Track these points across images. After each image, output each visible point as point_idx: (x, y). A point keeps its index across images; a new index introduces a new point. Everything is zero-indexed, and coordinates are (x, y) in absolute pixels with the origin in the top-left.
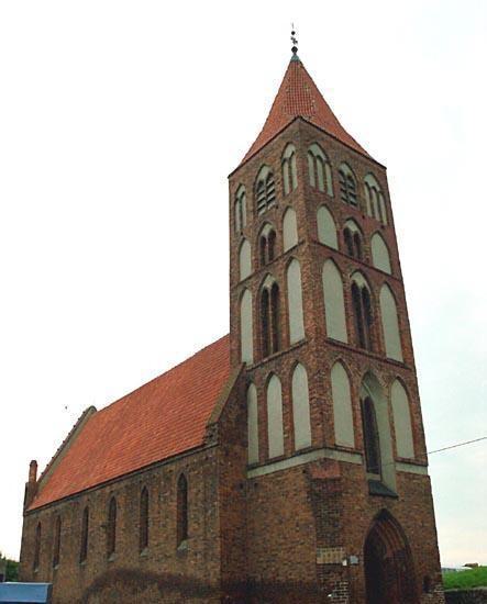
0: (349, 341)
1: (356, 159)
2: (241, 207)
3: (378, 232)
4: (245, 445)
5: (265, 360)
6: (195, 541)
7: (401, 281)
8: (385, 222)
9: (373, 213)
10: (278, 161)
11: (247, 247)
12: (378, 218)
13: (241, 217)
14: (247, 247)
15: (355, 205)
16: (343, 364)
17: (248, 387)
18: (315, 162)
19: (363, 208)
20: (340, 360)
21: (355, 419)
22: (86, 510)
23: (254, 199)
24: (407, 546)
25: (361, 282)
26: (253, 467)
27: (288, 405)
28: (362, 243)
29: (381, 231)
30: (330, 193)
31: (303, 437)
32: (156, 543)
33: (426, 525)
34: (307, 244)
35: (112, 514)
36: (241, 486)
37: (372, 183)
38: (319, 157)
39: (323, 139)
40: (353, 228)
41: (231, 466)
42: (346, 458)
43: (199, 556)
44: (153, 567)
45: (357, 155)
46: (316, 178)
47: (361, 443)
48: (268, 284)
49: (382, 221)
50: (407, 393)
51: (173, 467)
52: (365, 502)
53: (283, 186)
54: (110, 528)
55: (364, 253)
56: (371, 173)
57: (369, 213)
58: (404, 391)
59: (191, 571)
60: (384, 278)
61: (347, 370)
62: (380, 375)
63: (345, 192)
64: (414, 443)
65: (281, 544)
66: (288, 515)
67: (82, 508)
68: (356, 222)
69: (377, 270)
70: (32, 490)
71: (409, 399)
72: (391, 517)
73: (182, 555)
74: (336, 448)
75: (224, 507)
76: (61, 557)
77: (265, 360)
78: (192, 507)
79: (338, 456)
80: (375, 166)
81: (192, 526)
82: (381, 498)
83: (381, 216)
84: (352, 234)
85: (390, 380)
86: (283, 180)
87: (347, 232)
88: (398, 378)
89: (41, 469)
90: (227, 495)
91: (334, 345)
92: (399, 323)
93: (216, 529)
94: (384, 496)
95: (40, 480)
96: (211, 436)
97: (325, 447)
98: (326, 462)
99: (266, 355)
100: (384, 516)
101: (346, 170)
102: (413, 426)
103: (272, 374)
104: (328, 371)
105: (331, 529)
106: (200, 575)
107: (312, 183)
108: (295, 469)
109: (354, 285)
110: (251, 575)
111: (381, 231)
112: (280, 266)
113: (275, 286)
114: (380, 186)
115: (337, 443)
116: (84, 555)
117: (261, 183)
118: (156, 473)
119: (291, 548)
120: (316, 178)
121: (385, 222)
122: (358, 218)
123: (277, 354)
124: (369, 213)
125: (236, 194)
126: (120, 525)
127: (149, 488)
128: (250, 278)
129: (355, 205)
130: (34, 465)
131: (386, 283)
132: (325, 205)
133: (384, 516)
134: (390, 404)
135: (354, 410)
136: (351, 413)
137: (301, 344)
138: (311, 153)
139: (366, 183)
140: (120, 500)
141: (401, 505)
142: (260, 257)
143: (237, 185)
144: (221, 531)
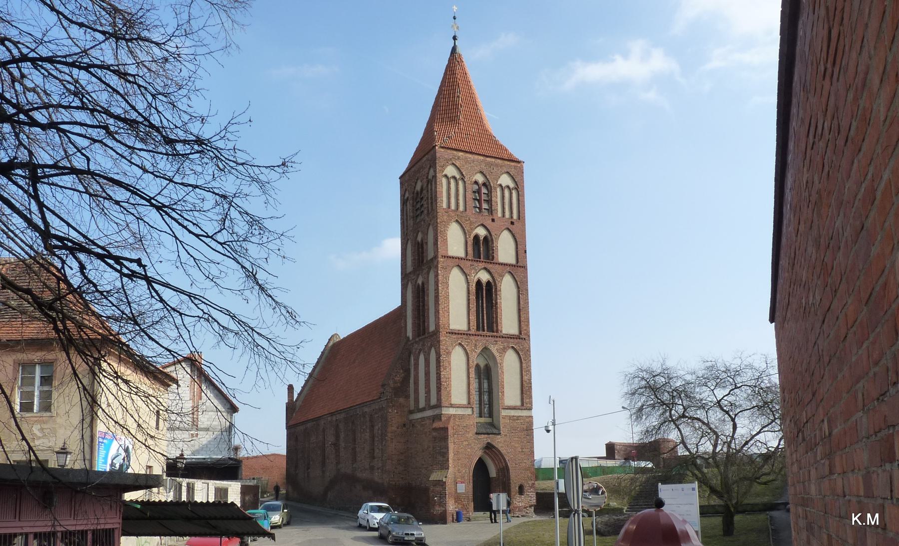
1: (490, 165)
5: (417, 340)
7: (525, 267)
9: (504, 212)
10: (425, 180)
16: (463, 346)
17: (410, 357)
18: (449, 183)
20: (460, 344)
22: (324, 431)
23: (413, 206)
25: (484, 277)
26: (411, 412)
27: (427, 374)
29: (511, 227)
30: (461, 208)
35: (337, 437)
37: (505, 180)
38: (454, 177)
39: (459, 158)
40: (481, 232)
41: (397, 413)
44: (359, 474)
45: (493, 160)
48: (420, 282)
49: (512, 217)
51: (366, 409)
53: (428, 204)
54: (336, 445)
56: (508, 173)
59: (376, 479)
60: (508, 269)
61: (465, 349)
62: (494, 349)
65: (423, 465)
66: (426, 447)
70: (291, 408)
72: (494, 447)
76: (311, 463)
78: (376, 439)
80: (513, 164)
81: (377, 451)
84: (482, 238)
85: (504, 350)
86: (428, 198)
88: (513, 347)
89: (297, 390)
91: (455, 333)
92: (519, 303)
94: (488, 434)
95: (296, 400)
99: (419, 336)
100: (489, 447)
103: (420, 350)
106: (380, 481)
108: (428, 418)
109: (479, 283)
111: (511, 227)
114: (516, 182)
115: (452, 403)
116: (323, 464)
117: (417, 193)
121: (515, 216)
122: (488, 223)
123: (423, 337)
124: (500, 214)
125: (404, 196)
126: (342, 444)
128: (410, 273)
130: (291, 388)
133: (489, 447)
138: (446, 176)
139: (501, 185)
140: (341, 426)
143: (404, 188)
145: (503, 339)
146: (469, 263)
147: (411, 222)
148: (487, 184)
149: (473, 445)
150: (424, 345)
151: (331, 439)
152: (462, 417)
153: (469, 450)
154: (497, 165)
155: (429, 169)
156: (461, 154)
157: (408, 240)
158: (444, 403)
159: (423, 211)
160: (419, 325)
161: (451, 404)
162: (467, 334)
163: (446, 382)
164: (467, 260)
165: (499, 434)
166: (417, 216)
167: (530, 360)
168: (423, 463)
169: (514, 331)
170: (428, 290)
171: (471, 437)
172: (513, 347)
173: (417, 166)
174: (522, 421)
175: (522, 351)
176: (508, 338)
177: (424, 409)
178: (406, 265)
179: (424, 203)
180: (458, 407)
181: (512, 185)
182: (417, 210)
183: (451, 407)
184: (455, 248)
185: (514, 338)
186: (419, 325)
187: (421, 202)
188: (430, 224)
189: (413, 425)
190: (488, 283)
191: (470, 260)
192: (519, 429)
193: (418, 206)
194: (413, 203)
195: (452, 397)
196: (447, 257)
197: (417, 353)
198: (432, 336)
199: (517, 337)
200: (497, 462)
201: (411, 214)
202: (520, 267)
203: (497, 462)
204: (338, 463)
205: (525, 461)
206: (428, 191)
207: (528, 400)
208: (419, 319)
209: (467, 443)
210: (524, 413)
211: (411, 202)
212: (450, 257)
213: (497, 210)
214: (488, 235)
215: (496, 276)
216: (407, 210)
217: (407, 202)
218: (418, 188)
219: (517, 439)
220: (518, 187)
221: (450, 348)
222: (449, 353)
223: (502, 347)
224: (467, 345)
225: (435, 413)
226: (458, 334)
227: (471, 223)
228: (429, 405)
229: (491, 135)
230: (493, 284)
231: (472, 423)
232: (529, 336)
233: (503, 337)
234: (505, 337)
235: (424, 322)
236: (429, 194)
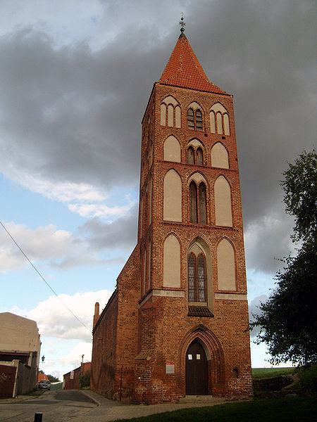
1: (202, 97)
12: (220, 132)
15: (202, 128)
16: (176, 235)
19: (207, 129)
25: (198, 178)
30: (178, 126)
40: (196, 144)
42: (172, 294)
57: (213, 131)
61: (178, 238)
62: (206, 238)
64: (236, 279)
71: (235, 251)
85: (218, 240)
88: (226, 238)
89: (102, 307)
101: (195, 106)
102: (236, 269)
105: (148, 338)
109: (193, 183)
121: (227, 133)
130: (97, 305)
132: (172, 135)
133: (201, 328)
135: (181, 263)
148: (201, 110)
152: (173, 300)
154: (209, 97)
156: (177, 88)
158: (155, 286)
161: (162, 287)
175: (235, 240)
184: (171, 156)
190: (202, 184)
210: (238, 297)
215: (209, 178)
222: (162, 241)
230: (206, 184)
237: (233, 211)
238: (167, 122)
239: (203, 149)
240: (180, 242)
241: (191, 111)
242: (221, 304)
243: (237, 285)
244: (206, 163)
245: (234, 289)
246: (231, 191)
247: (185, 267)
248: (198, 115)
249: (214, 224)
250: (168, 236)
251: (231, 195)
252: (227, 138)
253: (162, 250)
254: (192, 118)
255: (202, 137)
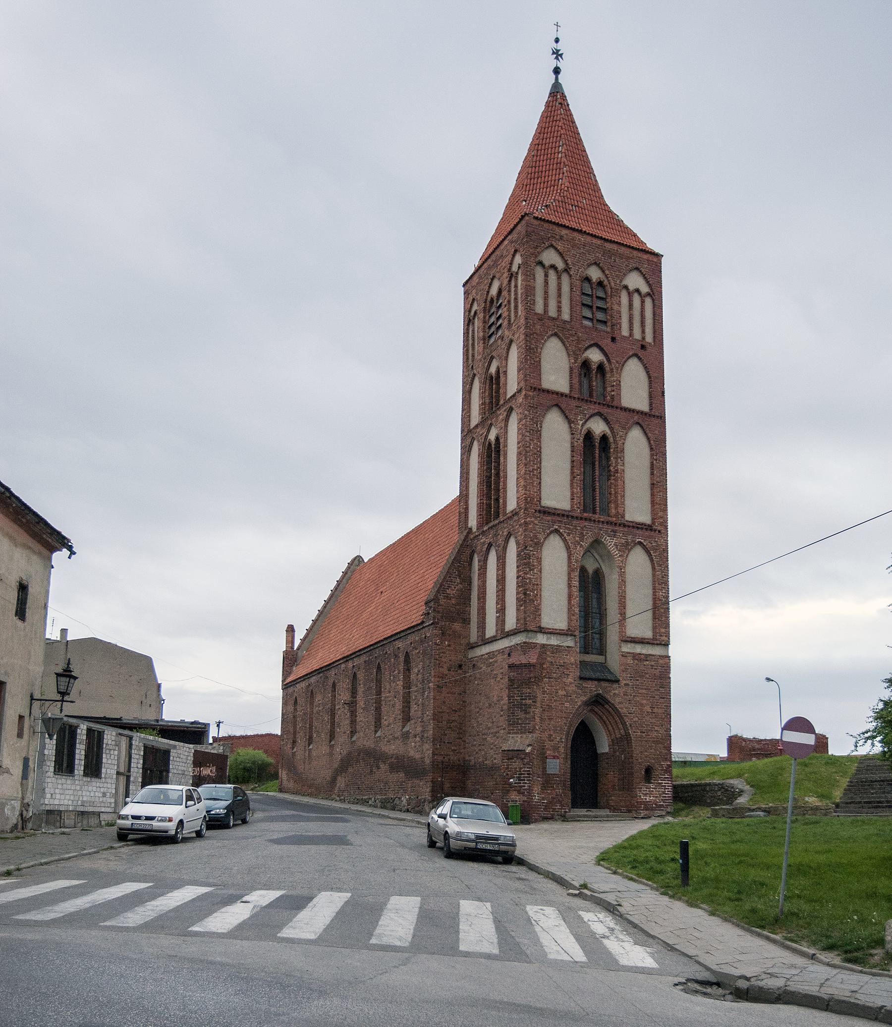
0: (572, 506)
2: (473, 330)
3: (636, 355)
4: (466, 621)
6: (416, 723)
7: (662, 418)
8: (649, 338)
11: (477, 384)
12: (637, 335)
13: (473, 345)
14: (477, 384)
15: (605, 323)
16: (561, 535)
19: (616, 326)
21: (570, 597)
22: (334, 685)
23: (484, 322)
24: (627, 735)
25: (598, 427)
26: (472, 647)
27: (501, 580)
28: (608, 375)
29: (641, 353)
31: (511, 622)
32: (386, 723)
33: (655, 710)
34: (524, 393)
35: (354, 692)
36: (460, 666)
37: (635, 281)
40: (595, 356)
41: (449, 645)
42: (554, 641)
43: (418, 739)
46: (546, 299)
47: (577, 623)
49: (644, 338)
50: (652, 560)
51: (399, 644)
52: (572, 688)
54: (352, 705)
55: (609, 389)
57: (625, 332)
58: (647, 558)
59: (412, 753)
61: (565, 540)
62: (610, 543)
63: (590, 307)
65: (489, 728)
66: (495, 698)
67: (330, 683)
68: (602, 350)
69: (626, 410)
70: (290, 659)
71: (654, 568)
72: (608, 702)
73: (406, 736)
74: (541, 630)
75: (439, 687)
77: (485, 529)
79: (541, 639)
80: (645, 257)
81: (414, 707)
82: (596, 682)
83: (643, 332)
84: (594, 367)
85: (626, 548)
87: (586, 364)
88: (640, 543)
90: (442, 677)
93: (429, 713)
94: (599, 680)
95: (298, 649)
96: (428, 614)
97: (526, 631)
98: (526, 647)
100: (598, 702)
103: (490, 545)
104: (539, 545)
106: (418, 756)
107: (539, 308)
108: (501, 652)
109: (589, 436)
110: (467, 758)
111: (641, 353)
112: (501, 417)
113: (497, 439)
114: (650, 286)
115: (543, 625)
116: (332, 736)
118: (389, 649)
119: (496, 733)
120: (546, 299)
121: (649, 338)
122: (606, 342)
123: (497, 522)
126: (361, 704)
127: (382, 666)
129: (605, 323)
131: (638, 423)
132: (556, 335)
133: (598, 702)
134: (622, 575)
135: (570, 586)
136: (566, 591)
137: (515, 513)
139: (626, 287)
140: (361, 676)
141: (622, 691)
142: (487, 401)
144: (434, 714)
145: (626, 529)
146: (574, 403)
147: (479, 347)
149: (574, 696)
150: (496, 535)
151: (344, 696)
152: (557, 649)
153: (567, 704)
155: (514, 256)
157: (474, 375)
159: (500, 325)
160: (489, 506)
161: (540, 627)
162: (568, 516)
163: (533, 591)
164: (570, 397)
165: (617, 681)
166: (490, 337)
167: (667, 567)
168: (490, 725)
169: (644, 517)
170: (506, 446)
171: (571, 683)
172: (640, 543)
173: (493, 257)
174: (653, 663)
175: (655, 550)
176: (633, 527)
177: (493, 640)
178: (469, 416)
179: (503, 311)
180: (551, 633)
181: (645, 289)
182: (490, 327)
183: (541, 632)
185: (642, 529)
186: (489, 506)
187: (497, 312)
188: (511, 341)
189: (474, 665)
190: (604, 438)
191: (574, 398)
192: (647, 676)
193: (493, 319)
194: (484, 317)
195: (542, 616)
196: (539, 389)
197: (484, 549)
198: (510, 518)
199: (649, 528)
200: (611, 728)
201: (481, 334)
202: (654, 416)
203: (611, 728)
204: (353, 733)
205: (656, 728)
206: (509, 291)
207: (663, 630)
208: (489, 498)
209: (564, 693)
210: (656, 651)
211: (481, 315)
212: (544, 391)
213: (620, 324)
214: (606, 362)
215: (616, 427)
216: (473, 330)
217: (474, 318)
218: (494, 291)
219: (644, 691)
220: (655, 294)
221: (541, 537)
223: (623, 541)
224: (569, 534)
225: (513, 644)
226: (554, 514)
227: (579, 341)
228: (503, 630)
229: (610, 212)
230: (611, 440)
231: (573, 660)
232: (666, 528)
233: (625, 526)
234: (629, 526)
235: (497, 500)
236: (513, 294)
237: (652, 495)
238: (546, 305)
239: (608, 369)
240: (568, 548)
241: (586, 285)
242: (630, 661)
243: (654, 628)
244: (613, 397)
245: (649, 634)
246: (652, 455)
247: (576, 592)
248: (601, 294)
249: (623, 516)
250: (549, 535)
251: (652, 464)
252: (649, 349)
253: (539, 560)
254: (588, 301)
255: (606, 342)
